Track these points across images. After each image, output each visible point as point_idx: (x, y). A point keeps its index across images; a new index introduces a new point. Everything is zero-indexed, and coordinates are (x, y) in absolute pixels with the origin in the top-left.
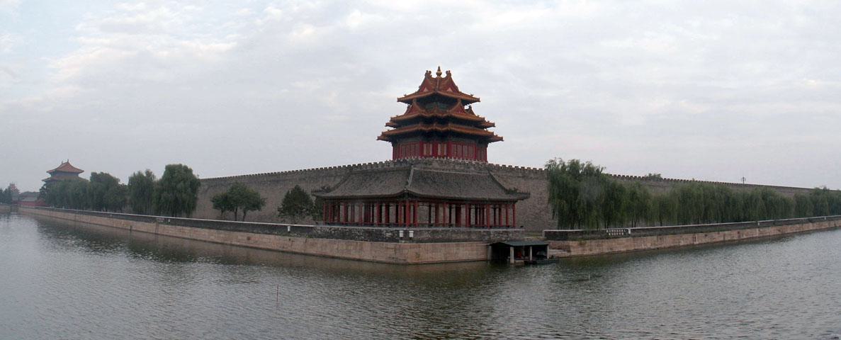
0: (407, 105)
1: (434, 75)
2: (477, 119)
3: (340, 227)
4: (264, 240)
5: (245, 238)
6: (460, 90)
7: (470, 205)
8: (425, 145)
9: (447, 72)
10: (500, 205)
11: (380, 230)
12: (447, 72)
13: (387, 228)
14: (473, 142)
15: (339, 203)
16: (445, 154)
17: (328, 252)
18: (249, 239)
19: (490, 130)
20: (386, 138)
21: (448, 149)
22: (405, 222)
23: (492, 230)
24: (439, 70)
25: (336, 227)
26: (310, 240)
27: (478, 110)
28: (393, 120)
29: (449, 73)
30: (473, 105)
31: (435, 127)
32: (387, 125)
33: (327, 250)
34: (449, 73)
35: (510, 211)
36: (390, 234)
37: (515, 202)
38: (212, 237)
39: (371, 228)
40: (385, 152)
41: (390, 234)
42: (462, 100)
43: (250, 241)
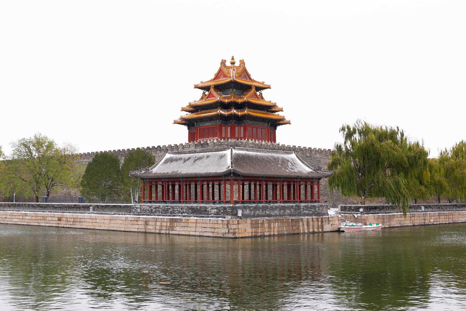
0: (201, 91)
1: (228, 64)
2: (268, 104)
3: (162, 205)
6: (252, 77)
7: (283, 182)
8: (223, 128)
9: (240, 61)
10: (306, 182)
11: (206, 208)
12: (240, 61)
13: (213, 205)
14: (266, 125)
15: (156, 182)
16: (242, 136)
18: (60, 219)
19: (280, 113)
20: (184, 122)
21: (245, 130)
22: (180, 199)
23: (303, 204)
24: (233, 59)
25: (157, 205)
27: (268, 97)
28: (190, 106)
29: (242, 62)
30: (263, 92)
31: (234, 111)
32: (183, 110)
34: (242, 62)
35: (316, 187)
36: (216, 210)
37: (319, 179)
39: (195, 205)
40: (182, 135)
41: (216, 210)
42: (255, 87)
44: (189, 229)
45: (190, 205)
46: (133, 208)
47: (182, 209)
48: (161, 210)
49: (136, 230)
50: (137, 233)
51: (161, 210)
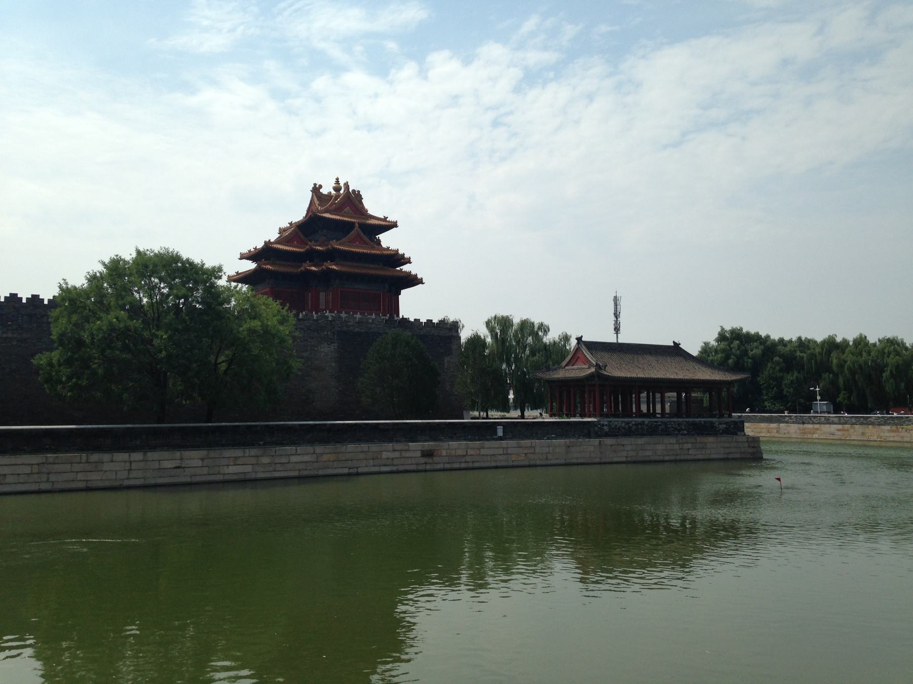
4: (483, 452)
5: (419, 454)
11: (712, 423)
17: (648, 454)
25: (640, 420)
26: (609, 441)
33: (648, 453)
38: (232, 469)
43: (436, 459)
44: (708, 451)
45: (691, 420)
46: (596, 426)
47: (679, 425)
48: (645, 428)
49: (624, 459)
50: (624, 466)
51: (645, 428)
